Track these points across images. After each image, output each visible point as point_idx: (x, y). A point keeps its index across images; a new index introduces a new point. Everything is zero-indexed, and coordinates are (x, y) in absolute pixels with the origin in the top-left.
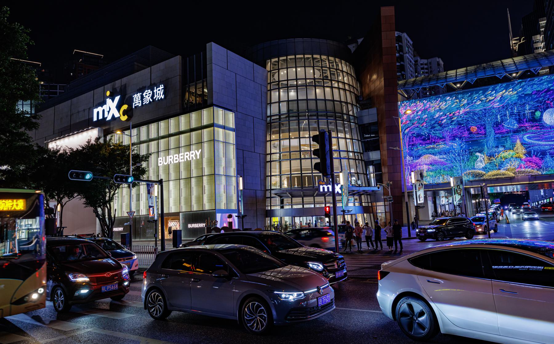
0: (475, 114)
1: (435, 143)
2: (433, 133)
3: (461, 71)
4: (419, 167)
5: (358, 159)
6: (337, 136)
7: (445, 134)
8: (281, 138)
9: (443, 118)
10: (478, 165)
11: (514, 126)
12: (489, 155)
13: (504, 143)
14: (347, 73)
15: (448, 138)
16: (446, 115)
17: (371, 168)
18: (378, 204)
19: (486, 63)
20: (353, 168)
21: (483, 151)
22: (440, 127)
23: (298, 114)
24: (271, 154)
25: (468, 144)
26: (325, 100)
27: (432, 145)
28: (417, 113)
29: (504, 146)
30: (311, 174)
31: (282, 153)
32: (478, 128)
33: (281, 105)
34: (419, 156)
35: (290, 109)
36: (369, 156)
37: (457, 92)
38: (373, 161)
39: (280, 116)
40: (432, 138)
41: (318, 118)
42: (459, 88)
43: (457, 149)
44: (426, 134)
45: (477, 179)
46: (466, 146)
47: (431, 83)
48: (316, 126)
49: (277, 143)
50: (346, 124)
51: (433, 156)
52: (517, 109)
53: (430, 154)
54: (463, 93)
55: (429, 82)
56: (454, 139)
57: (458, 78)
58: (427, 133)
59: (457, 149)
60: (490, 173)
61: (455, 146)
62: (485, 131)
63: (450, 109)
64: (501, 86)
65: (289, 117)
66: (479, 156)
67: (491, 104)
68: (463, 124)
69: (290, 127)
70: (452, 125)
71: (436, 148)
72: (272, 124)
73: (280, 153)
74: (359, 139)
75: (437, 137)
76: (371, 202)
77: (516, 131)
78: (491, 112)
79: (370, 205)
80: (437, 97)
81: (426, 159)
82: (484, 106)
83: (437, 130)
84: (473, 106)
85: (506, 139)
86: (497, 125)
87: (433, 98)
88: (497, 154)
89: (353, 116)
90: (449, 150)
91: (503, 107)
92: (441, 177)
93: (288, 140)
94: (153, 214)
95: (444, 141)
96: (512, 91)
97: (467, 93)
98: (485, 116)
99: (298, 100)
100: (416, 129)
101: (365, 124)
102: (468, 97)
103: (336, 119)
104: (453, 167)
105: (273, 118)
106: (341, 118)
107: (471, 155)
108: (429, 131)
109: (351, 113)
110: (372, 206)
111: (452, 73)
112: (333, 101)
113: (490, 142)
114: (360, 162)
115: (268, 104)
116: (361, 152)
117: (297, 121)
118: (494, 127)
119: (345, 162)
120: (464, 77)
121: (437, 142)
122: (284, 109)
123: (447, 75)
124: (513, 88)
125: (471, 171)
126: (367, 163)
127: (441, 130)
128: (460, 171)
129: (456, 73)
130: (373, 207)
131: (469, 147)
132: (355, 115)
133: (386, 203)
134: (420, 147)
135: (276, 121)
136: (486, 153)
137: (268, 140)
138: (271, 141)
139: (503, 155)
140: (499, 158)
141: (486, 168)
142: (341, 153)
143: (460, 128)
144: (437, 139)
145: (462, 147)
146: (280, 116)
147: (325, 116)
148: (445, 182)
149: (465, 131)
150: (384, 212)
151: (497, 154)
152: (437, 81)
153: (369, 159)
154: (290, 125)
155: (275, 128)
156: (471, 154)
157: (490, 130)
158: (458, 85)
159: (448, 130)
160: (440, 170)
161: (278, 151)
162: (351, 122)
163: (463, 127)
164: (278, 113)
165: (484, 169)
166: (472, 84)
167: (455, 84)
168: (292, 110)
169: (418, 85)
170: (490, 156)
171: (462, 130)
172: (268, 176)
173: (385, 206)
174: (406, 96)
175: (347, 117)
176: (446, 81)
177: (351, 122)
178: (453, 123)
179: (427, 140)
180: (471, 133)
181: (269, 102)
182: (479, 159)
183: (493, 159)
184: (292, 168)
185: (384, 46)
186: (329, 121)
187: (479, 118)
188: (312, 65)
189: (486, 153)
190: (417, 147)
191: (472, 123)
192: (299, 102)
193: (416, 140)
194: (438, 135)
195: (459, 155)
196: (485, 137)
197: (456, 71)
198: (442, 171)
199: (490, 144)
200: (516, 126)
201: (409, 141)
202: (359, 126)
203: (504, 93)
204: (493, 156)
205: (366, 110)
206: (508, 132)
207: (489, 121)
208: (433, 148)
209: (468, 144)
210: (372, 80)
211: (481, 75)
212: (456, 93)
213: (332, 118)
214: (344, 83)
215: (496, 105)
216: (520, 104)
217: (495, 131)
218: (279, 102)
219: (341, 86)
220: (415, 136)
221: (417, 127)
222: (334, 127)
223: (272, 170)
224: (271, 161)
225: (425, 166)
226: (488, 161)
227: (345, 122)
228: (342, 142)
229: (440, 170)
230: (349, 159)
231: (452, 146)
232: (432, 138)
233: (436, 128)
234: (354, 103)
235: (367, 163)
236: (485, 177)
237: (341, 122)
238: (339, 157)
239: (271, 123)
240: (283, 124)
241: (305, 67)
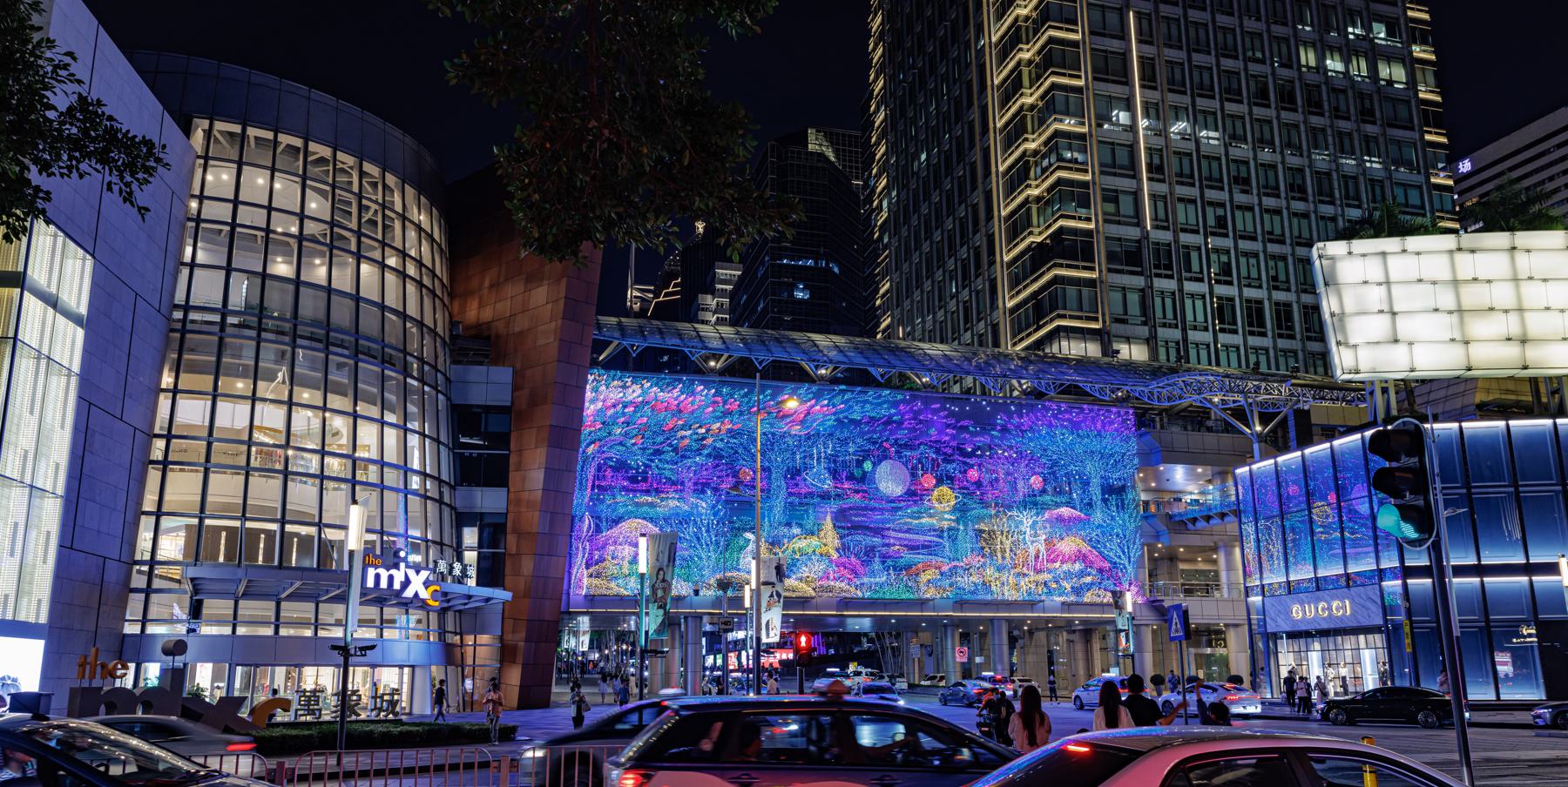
1: (658, 491)
2: (657, 466)
4: (613, 548)
9: (684, 433)
11: (824, 482)
12: (771, 540)
13: (803, 519)
16: (690, 429)
25: (731, 509)
27: (650, 496)
28: (625, 407)
29: (800, 525)
34: (617, 521)
46: (725, 513)
51: (650, 525)
52: (834, 447)
53: (644, 518)
56: (703, 492)
58: (644, 463)
64: (808, 389)
67: (787, 424)
70: (700, 454)
75: (666, 478)
77: (825, 496)
80: (675, 380)
82: (772, 425)
85: (806, 511)
86: (794, 474)
88: (786, 540)
90: (688, 516)
91: (808, 437)
96: (828, 406)
97: (742, 386)
100: (620, 448)
102: (743, 397)
113: (776, 511)
118: (786, 477)
121: (662, 492)
124: (830, 400)
127: (676, 463)
131: (731, 516)
139: (801, 544)
140: (790, 550)
143: (717, 466)
144: (665, 484)
149: (727, 475)
151: (786, 540)
157: (779, 483)
170: (772, 544)
178: (706, 452)
179: (639, 481)
183: (778, 550)
190: (614, 496)
193: (613, 477)
194: (667, 473)
200: (828, 485)
201: (597, 477)
203: (814, 406)
206: (811, 495)
208: (652, 505)
209: (731, 509)
215: (796, 429)
216: (839, 439)
217: (788, 488)
220: (611, 467)
221: (621, 444)
225: (627, 547)
231: (697, 507)
233: (667, 457)
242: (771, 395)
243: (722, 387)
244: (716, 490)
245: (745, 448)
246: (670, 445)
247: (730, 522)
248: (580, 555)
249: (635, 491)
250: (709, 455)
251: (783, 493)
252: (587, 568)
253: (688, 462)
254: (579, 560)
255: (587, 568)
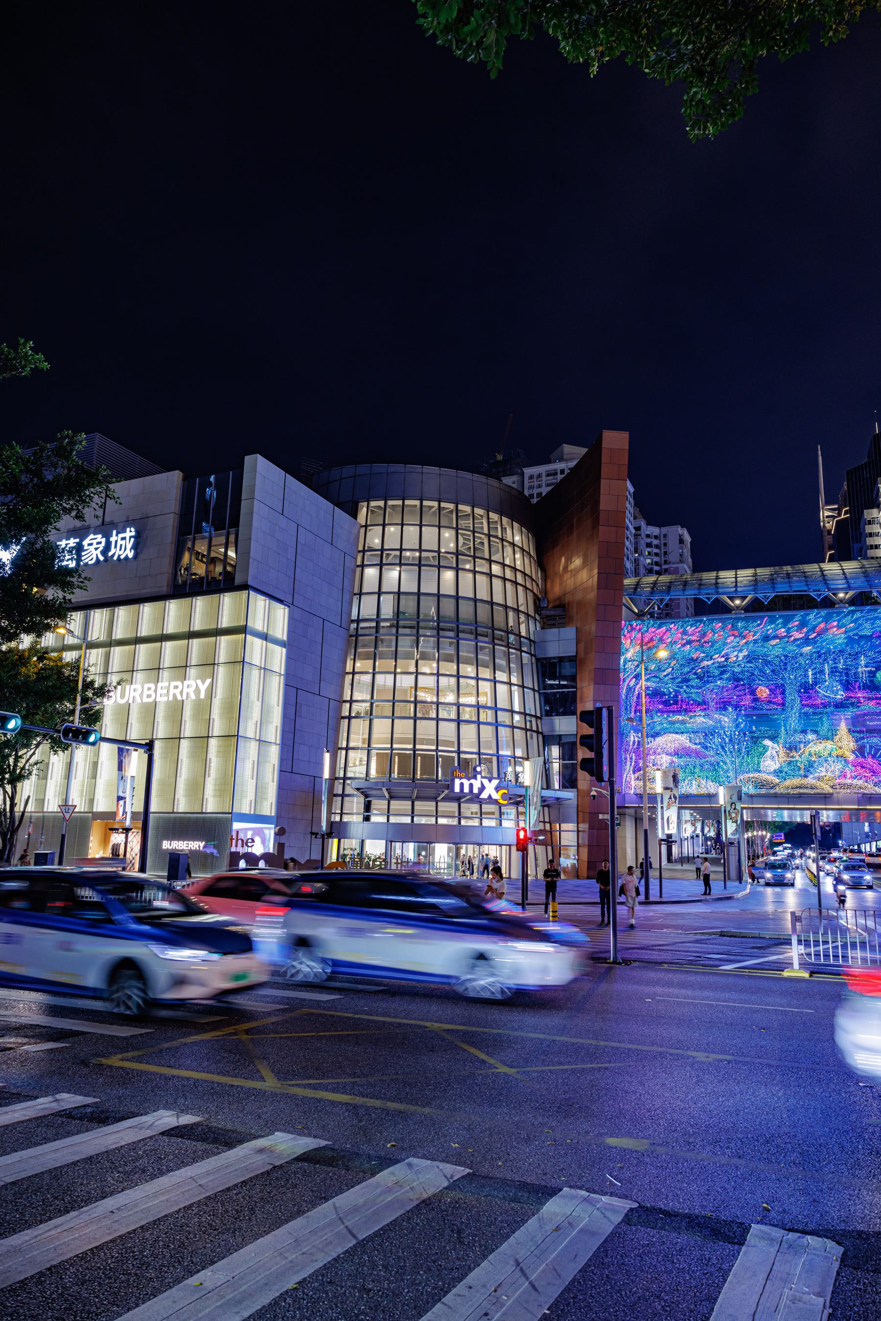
0: (767, 663)
1: (687, 711)
2: (685, 691)
3: (744, 575)
4: (653, 757)
5: (531, 730)
6: (492, 678)
7: (709, 697)
8: (377, 670)
10: (766, 763)
12: (787, 746)
14: (522, 550)
15: (712, 704)
16: (711, 659)
17: (555, 751)
18: (564, 826)
19: (792, 563)
20: (519, 747)
21: (777, 737)
22: (698, 681)
23: (418, 623)
24: (351, 702)
26: (475, 600)
27: (681, 715)
30: (434, 753)
31: (377, 701)
32: (770, 690)
33: (381, 598)
34: (655, 735)
35: (401, 610)
36: (552, 725)
37: (733, 617)
38: (560, 736)
39: (378, 623)
40: (682, 701)
41: (458, 636)
42: (738, 607)
43: (728, 728)
44: (670, 693)
45: (763, 791)
46: (746, 724)
47: (687, 593)
48: (452, 651)
49: (368, 678)
50: (513, 654)
53: (677, 733)
54: (746, 619)
55: (684, 590)
56: (725, 709)
57: (739, 589)
59: (728, 728)
60: (788, 783)
61: (725, 722)
62: (784, 698)
63: (720, 647)
65: (397, 627)
66: (768, 746)
68: (742, 680)
69: (399, 649)
70: (721, 679)
71: (689, 723)
72: (360, 638)
73: (373, 701)
74: (536, 688)
75: (693, 700)
76: (550, 823)
78: (796, 663)
79: (548, 827)
80: (697, 621)
81: (669, 741)
82: (784, 649)
83: (692, 686)
84: (765, 647)
87: (689, 621)
89: (529, 639)
92: (694, 782)
93: (393, 676)
94: (123, 815)
95: (705, 709)
97: (755, 619)
98: (786, 669)
99: (419, 594)
101: (550, 658)
103: (493, 641)
104: (718, 763)
105: (362, 625)
106: (502, 641)
107: (755, 743)
108: (678, 687)
109: (523, 633)
110: (551, 832)
111: (727, 576)
112: (492, 603)
114: (535, 735)
115: (355, 594)
116: (539, 715)
117: (415, 638)
118: (799, 692)
119: (504, 732)
120: (751, 588)
122: (388, 609)
123: (719, 581)
125: (752, 775)
126: (548, 740)
127: (701, 688)
128: (731, 774)
129: (736, 578)
130: (553, 833)
132: (532, 637)
133: (581, 825)
134: (657, 718)
135: (367, 632)
136: (782, 741)
137: (347, 671)
138: (354, 673)
141: (781, 772)
142: (499, 712)
143: (737, 687)
144: (692, 705)
145: (737, 726)
146: (378, 623)
147: (471, 633)
148: (702, 792)
149: (745, 694)
150: (576, 844)
152: (699, 589)
153: (553, 730)
154: (399, 644)
155: (365, 646)
156: (755, 740)
157: (792, 696)
158: (738, 602)
159: (713, 689)
160: (694, 767)
161: (368, 697)
162: (522, 651)
163: (743, 685)
164: (375, 617)
165: (778, 773)
166: (766, 603)
167: (732, 599)
168: (404, 613)
169: (661, 592)
171: (741, 691)
172: (341, 749)
173: (578, 831)
174: (636, 611)
175: (515, 639)
176: (717, 593)
177: (522, 651)
180: (756, 700)
181: (356, 591)
182: (768, 753)
184: (395, 736)
185: (602, 507)
186: (479, 644)
187: (773, 671)
188: (454, 526)
189: (782, 741)
191: (759, 680)
192: (422, 597)
193: (650, 702)
195: (731, 740)
196: (783, 709)
197: (736, 575)
198: (697, 770)
199: (791, 724)
202: (538, 660)
204: (796, 751)
205: (555, 630)
207: (790, 678)
208: (683, 722)
210: (571, 571)
211: (782, 588)
212: (732, 618)
213: (486, 639)
214: (514, 569)
217: (801, 701)
218: (380, 593)
219: (509, 574)
222: (488, 658)
223: (352, 736)
224: (350, 718)
225: (664, 756)
226: (785, 759)
227: (511, 650)
228: (502, 689)
229: (694, 767)
230: (513, 727)
231: (720, 721)
232: (682, 701)
234: (531, 612)
235: (548, 740)
236: (777, 790)
237: (504, 648)
238: (494, 722)
239: (357, 636)
240: (382, 640)
241: (439, 527)
242: (781, 624)
243: (738, 622)
244: (736, 707)
245: (760, 670)
246: (695, 674)
247: (750, 732)
248: (628, 763)
249: (669, 712)
250: (729, 679)
251: (797, 705)
252: (634, 773)
253: (711, 686)
254: (629, 767)
255: (634, 773)
